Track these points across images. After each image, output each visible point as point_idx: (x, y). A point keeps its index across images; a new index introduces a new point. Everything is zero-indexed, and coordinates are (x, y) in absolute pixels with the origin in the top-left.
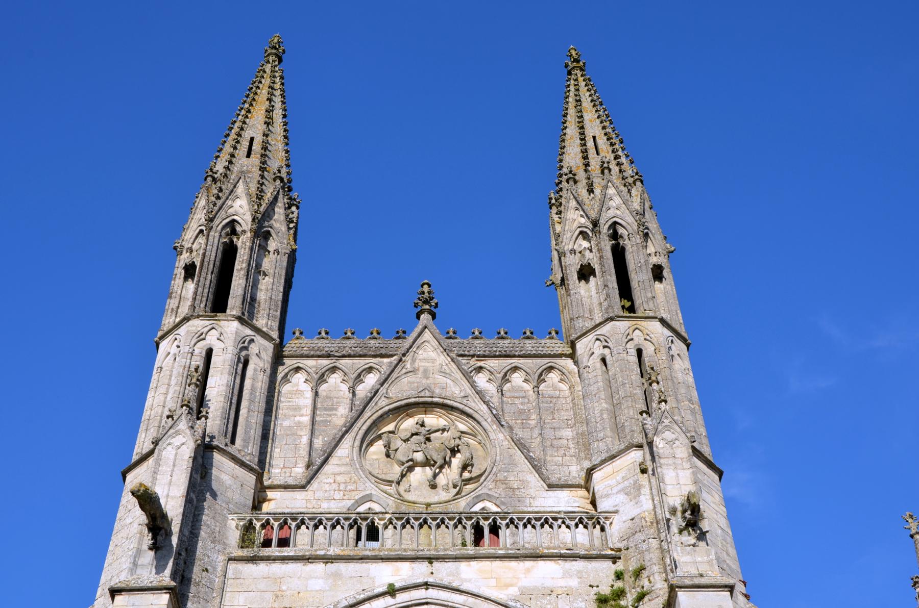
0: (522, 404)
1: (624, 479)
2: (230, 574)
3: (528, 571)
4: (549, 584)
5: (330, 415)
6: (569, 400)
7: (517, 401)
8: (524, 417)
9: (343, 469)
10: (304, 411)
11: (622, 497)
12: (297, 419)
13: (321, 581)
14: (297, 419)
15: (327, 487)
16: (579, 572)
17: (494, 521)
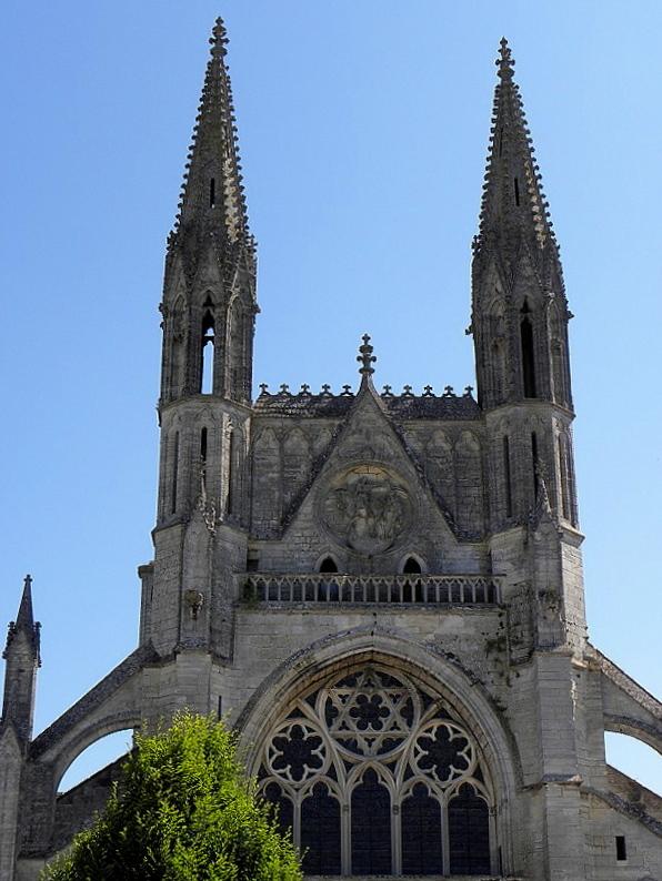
0: (442, 463)
1: (513, 551)
2: (239, 620)
3: (441, 622)
4: (455, 632)
5: (295, 472)
6: (479, 460)
7: (438, 461)
8: (442, 476)
9: (308, 525)
10: (275, 468)
11: (509, 565)
12: (270, 475)
13: (301, 628)
14: (270, 475)
15: (297, 540)
16: (476, 623)
17: (419, 581)
